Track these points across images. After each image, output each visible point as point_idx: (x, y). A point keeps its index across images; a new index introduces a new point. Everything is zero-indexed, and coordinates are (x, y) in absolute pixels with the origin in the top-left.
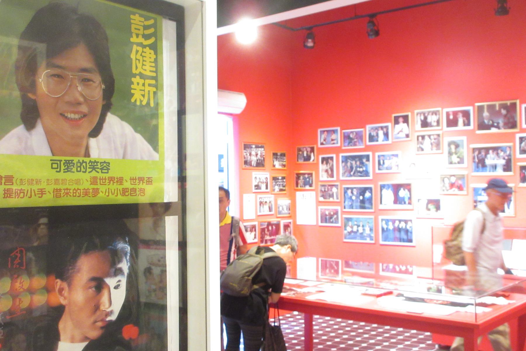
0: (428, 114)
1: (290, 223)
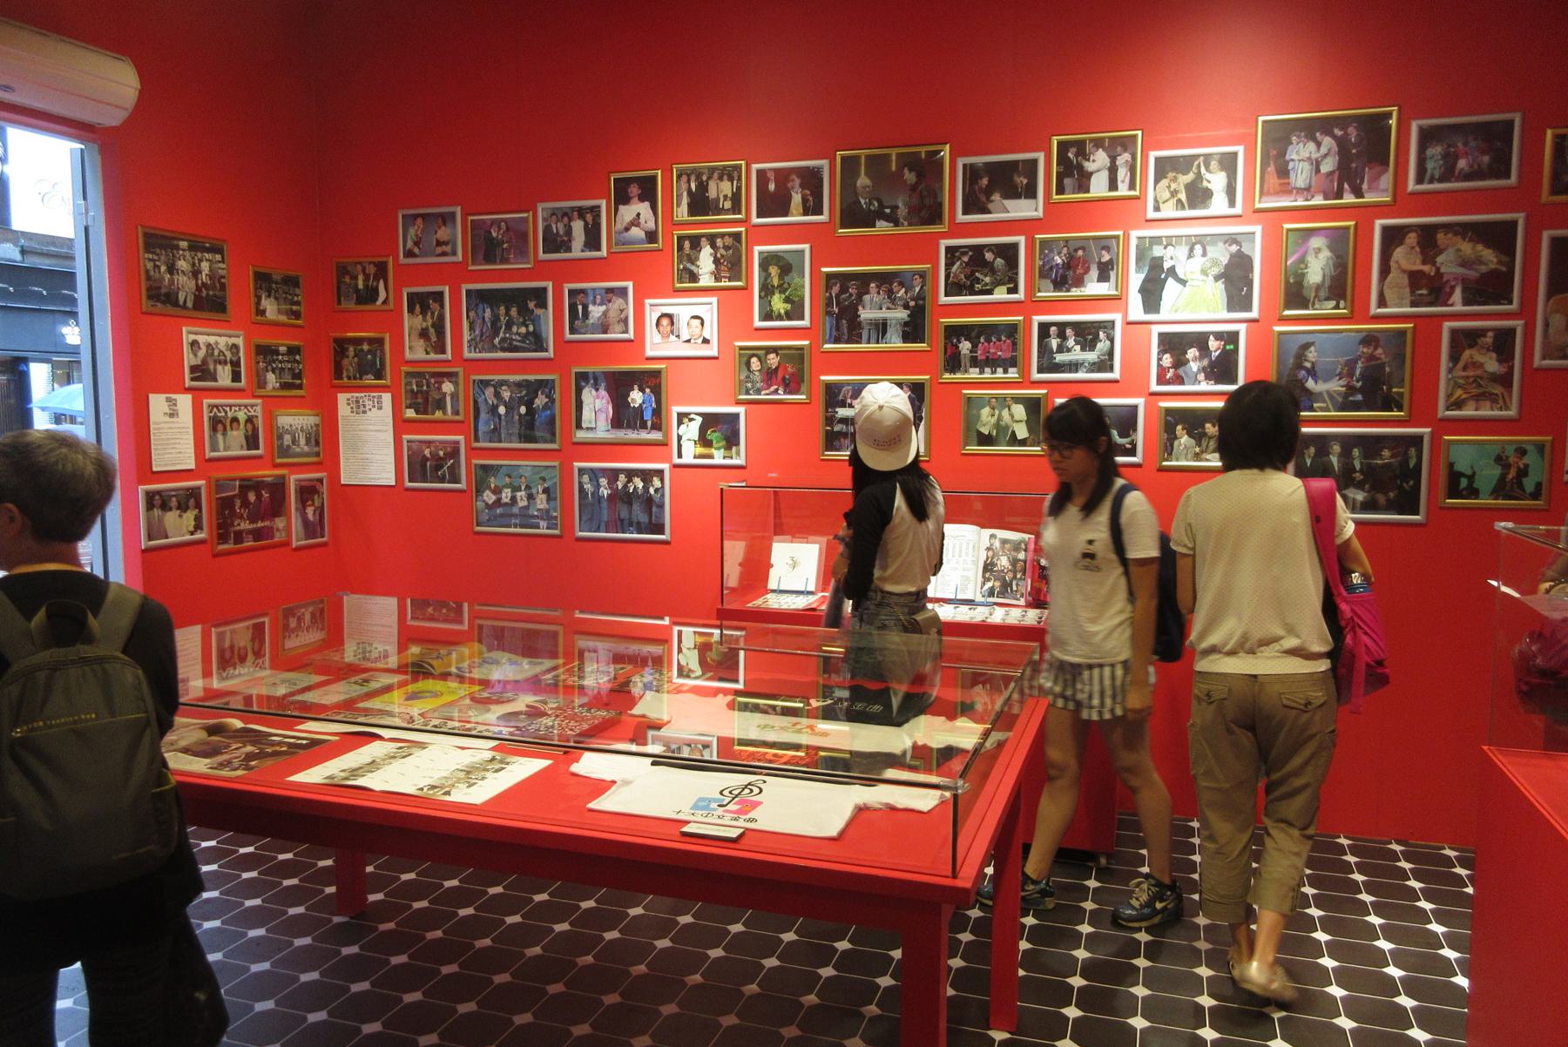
0: (709, 178)
1: (320, 481)
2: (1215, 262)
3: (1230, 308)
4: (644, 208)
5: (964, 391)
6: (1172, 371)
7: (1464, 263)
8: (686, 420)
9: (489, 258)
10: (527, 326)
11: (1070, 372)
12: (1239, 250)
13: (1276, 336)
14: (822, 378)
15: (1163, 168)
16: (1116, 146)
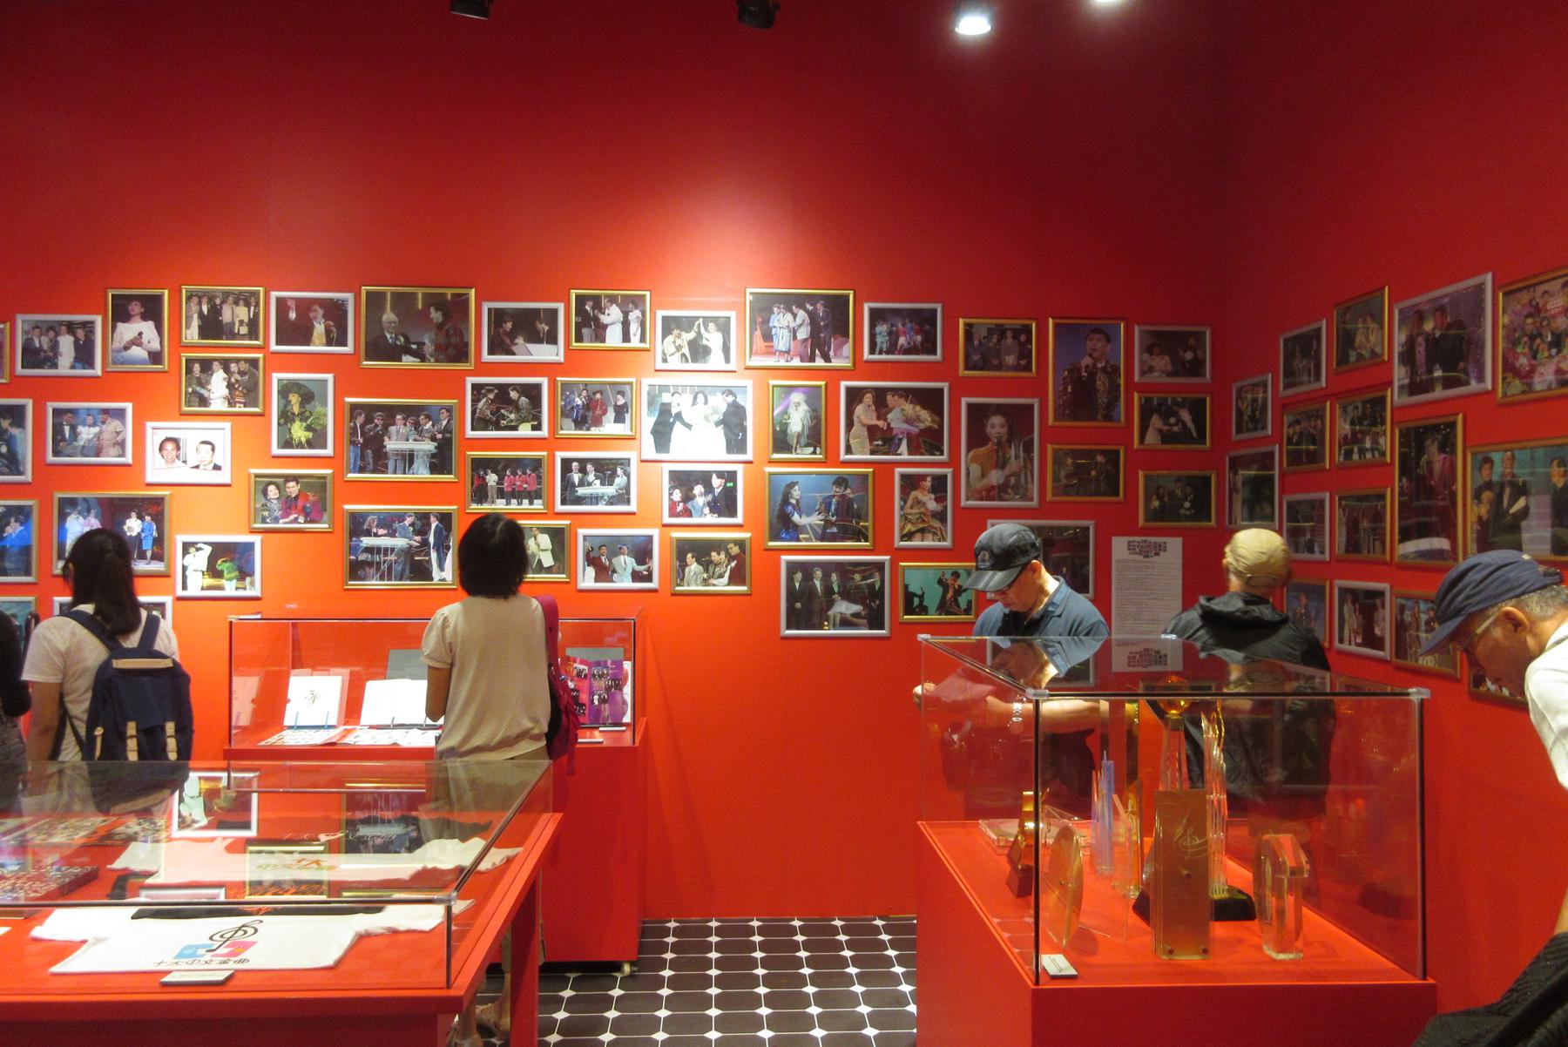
0: (223, 302)
2: (715, 411)
3: (730, 450)
4: (148, 328)
6: (681, 504)
7: (908, 421)
8: (192, 550)
12: (735, 401)
13: (767, 476)
14: (347, 507)
15: (670, 325)
16: (629, 303)
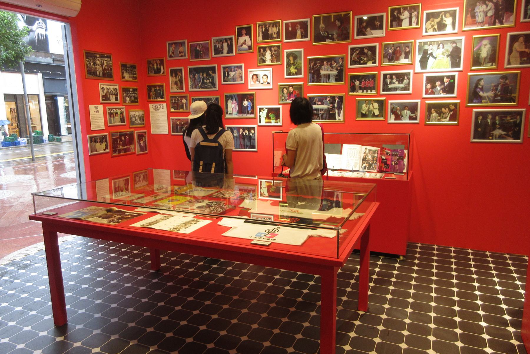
1: (145, 133)
2: (447, 51)
4: (247, 38)
5: (357, 99)
6: (430, 90)
8: (262, 110)
9: (197, 57)
10: (209, 80)
11: (394, 91)
12: (456, 46)
13: (469, 77)
